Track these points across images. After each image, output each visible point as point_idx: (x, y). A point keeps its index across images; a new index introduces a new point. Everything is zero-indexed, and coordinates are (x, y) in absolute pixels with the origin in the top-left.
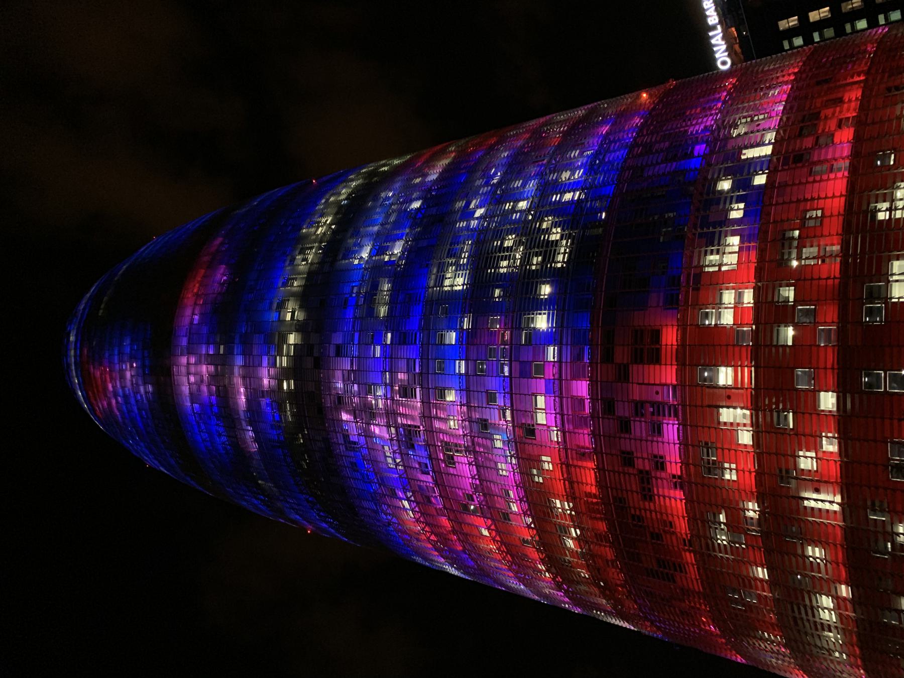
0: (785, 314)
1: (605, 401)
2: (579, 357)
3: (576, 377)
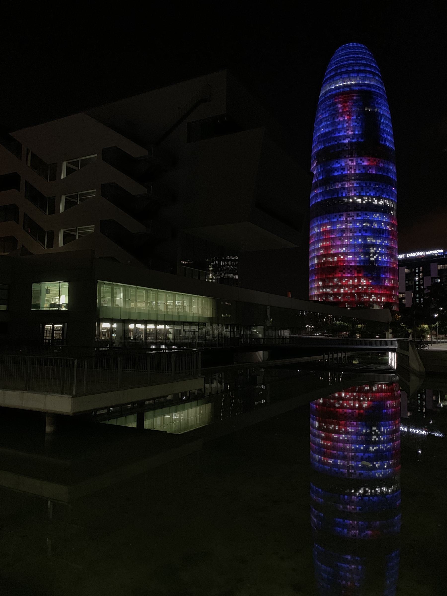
0: (363, 287)
1: (351, 266)
2: (357, 263)
3: (355, 263)
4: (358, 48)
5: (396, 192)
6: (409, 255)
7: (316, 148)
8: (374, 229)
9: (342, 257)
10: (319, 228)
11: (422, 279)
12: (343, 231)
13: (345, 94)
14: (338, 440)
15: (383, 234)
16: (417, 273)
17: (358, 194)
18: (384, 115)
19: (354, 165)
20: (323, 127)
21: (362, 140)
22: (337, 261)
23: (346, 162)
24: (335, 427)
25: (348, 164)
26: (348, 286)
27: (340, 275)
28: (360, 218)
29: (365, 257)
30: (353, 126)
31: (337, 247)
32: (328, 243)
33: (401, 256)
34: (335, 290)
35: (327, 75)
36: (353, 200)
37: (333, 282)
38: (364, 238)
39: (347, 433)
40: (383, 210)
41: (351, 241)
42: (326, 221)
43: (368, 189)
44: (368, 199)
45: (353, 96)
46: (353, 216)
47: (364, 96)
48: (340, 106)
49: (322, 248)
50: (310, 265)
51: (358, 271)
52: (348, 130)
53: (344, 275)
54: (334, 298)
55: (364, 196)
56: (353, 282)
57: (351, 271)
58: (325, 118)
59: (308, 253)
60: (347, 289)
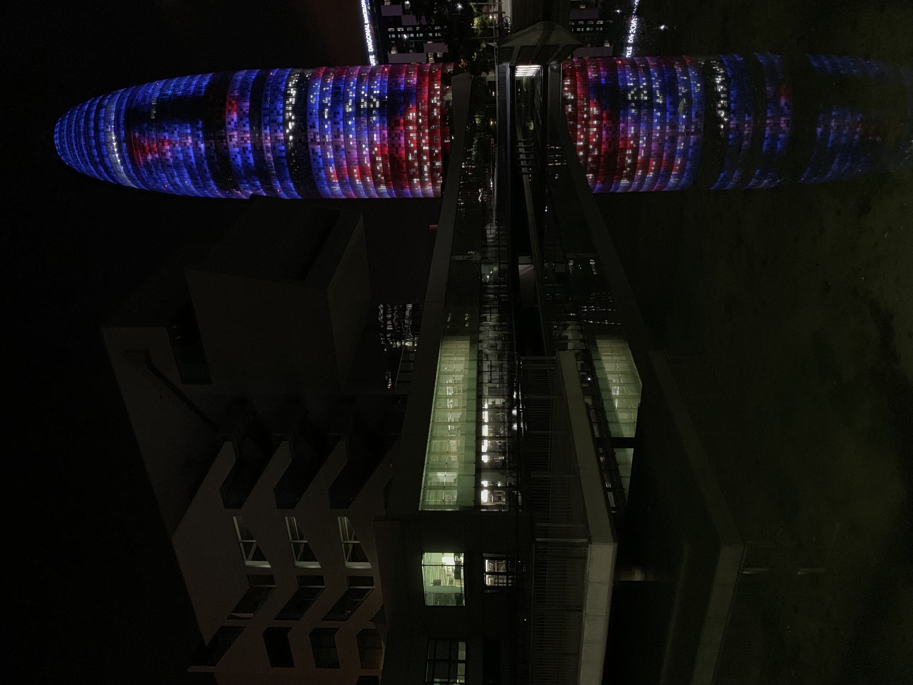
0: (420, 117)
1: (389, 135)
4: (61, 131)
5: (276, 71)
6: (371, 48)
7: (214, 191)
8: (332, 102)
9: (376, 149)
10: (334, 184)
11: (405, 29)
12: (336, 149)
13: (131, 149)
14: (648, 150)
15: (340, 88)
16: (397, 36)
17: (281, 128)
18: (161, 90)
19: (238, 135)
20: (182, 181)
21: (200, 123)
22: (383, 156)
23: (234, 146)
24: (629, 155)
26: (419, 139)
27: (403, 152)
28: (317, 123)
29: (375, 115)
31: (360, 157)
32: (355, 171)
33: (373, 60)
34: (425, 158)
35: (104, 178)
36: (290, 134)
37: (413, 162)
38: (347, 116)
39: (636, 137)
40: (304, 89)
41: (351, 136)
42: (323, 174)
43: (272, 112)
44: (288, 111)
45: (134, 137)
46: (314, 133)
47: (134, 121)
48: (150, 157)
49: (362, 179)
50: (388, 197)
51: (396, 125)
52: (185, 144)
53: (403, 145)
54: (437, 160)
55: (284, 118)
56: (412, 132)
58: (168, 180)
59: (371, 200)
60: (423, 141)
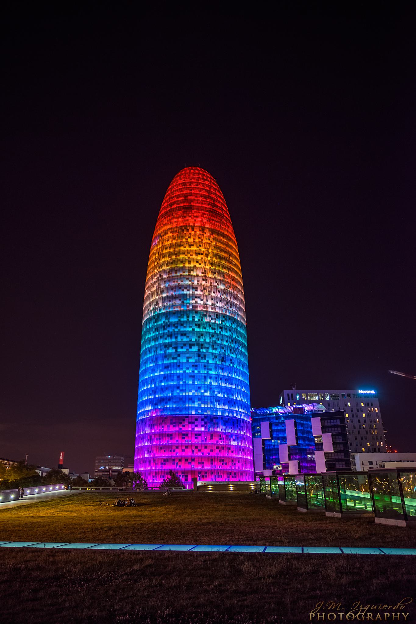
1: (206, 417)
3: (210, 412)
25: (201, 284)
30: (207, 243)
46: (208, 348)
51: (214, 423)
52: (200, 246)
57: (205, 423)
